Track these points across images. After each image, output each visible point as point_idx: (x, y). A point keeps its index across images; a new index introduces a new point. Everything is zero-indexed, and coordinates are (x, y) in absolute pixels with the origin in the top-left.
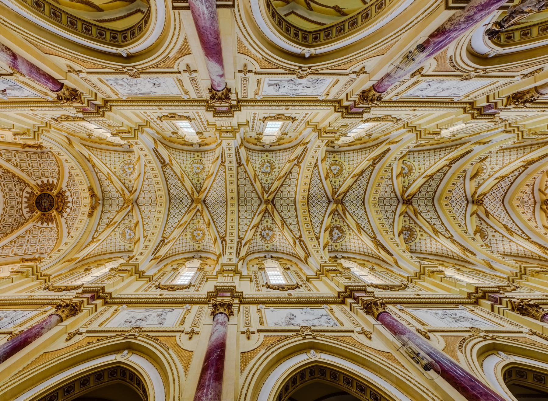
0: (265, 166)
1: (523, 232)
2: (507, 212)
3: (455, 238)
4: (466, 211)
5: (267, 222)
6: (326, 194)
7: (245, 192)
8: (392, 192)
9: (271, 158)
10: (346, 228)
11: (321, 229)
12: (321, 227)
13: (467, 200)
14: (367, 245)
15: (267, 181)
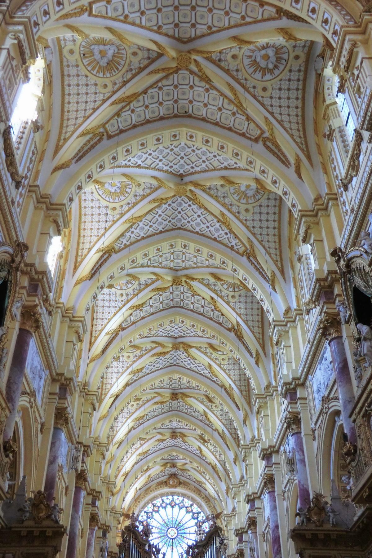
1: (142, 460)
3: (133, 431)
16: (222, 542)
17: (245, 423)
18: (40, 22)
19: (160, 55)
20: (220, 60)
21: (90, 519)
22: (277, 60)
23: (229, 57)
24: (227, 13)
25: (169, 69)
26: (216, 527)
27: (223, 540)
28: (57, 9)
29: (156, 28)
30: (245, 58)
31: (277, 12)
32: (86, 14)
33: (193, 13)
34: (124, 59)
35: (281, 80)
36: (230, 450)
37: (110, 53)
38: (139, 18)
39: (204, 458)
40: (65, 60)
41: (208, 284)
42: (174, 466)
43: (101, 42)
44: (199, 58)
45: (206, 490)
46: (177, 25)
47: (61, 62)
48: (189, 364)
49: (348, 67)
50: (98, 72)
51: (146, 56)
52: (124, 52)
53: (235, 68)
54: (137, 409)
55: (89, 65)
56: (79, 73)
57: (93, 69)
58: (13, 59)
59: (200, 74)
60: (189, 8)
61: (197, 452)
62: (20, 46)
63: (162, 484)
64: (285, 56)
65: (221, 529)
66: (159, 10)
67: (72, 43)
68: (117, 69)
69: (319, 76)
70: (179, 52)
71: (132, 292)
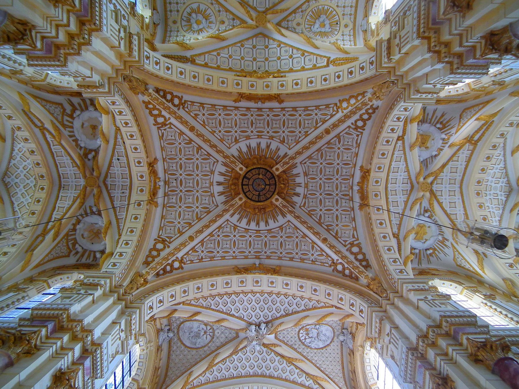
18: (368, 64)
19: (279, 24)
20: (234, 19)
22: (190, 20)
23: (227, 23)
24: (230, 57)
25: (273, 13)
28: (353, 69)
29: (282, 45)
30: (214, 22)
31: (194, 61)
32: (331, 59)
33: (255, 56)
34: (306, 20)
35: (184, 3)
37: (317, 26)
38: (294, 53)
40: (352, 20)
43: (324, 34)
44: (250, 22)
46: (267, 47)
47: (355, 18)
49: (130, 37)
50: (328, 10)
51: (290, 23)
52: (306, 26)
53: (221, 13)
55: (335, 16)
56: (342, 8)
57: (332, 12)
58: (397, 45)
59: (249, 9)
60: (258, 60)
62: (389, 54)
64: (184, 23)
66: (279, 58)
67: (345, 33)
68: (313, 12)
69: (154, 9)
70: (266, 28)
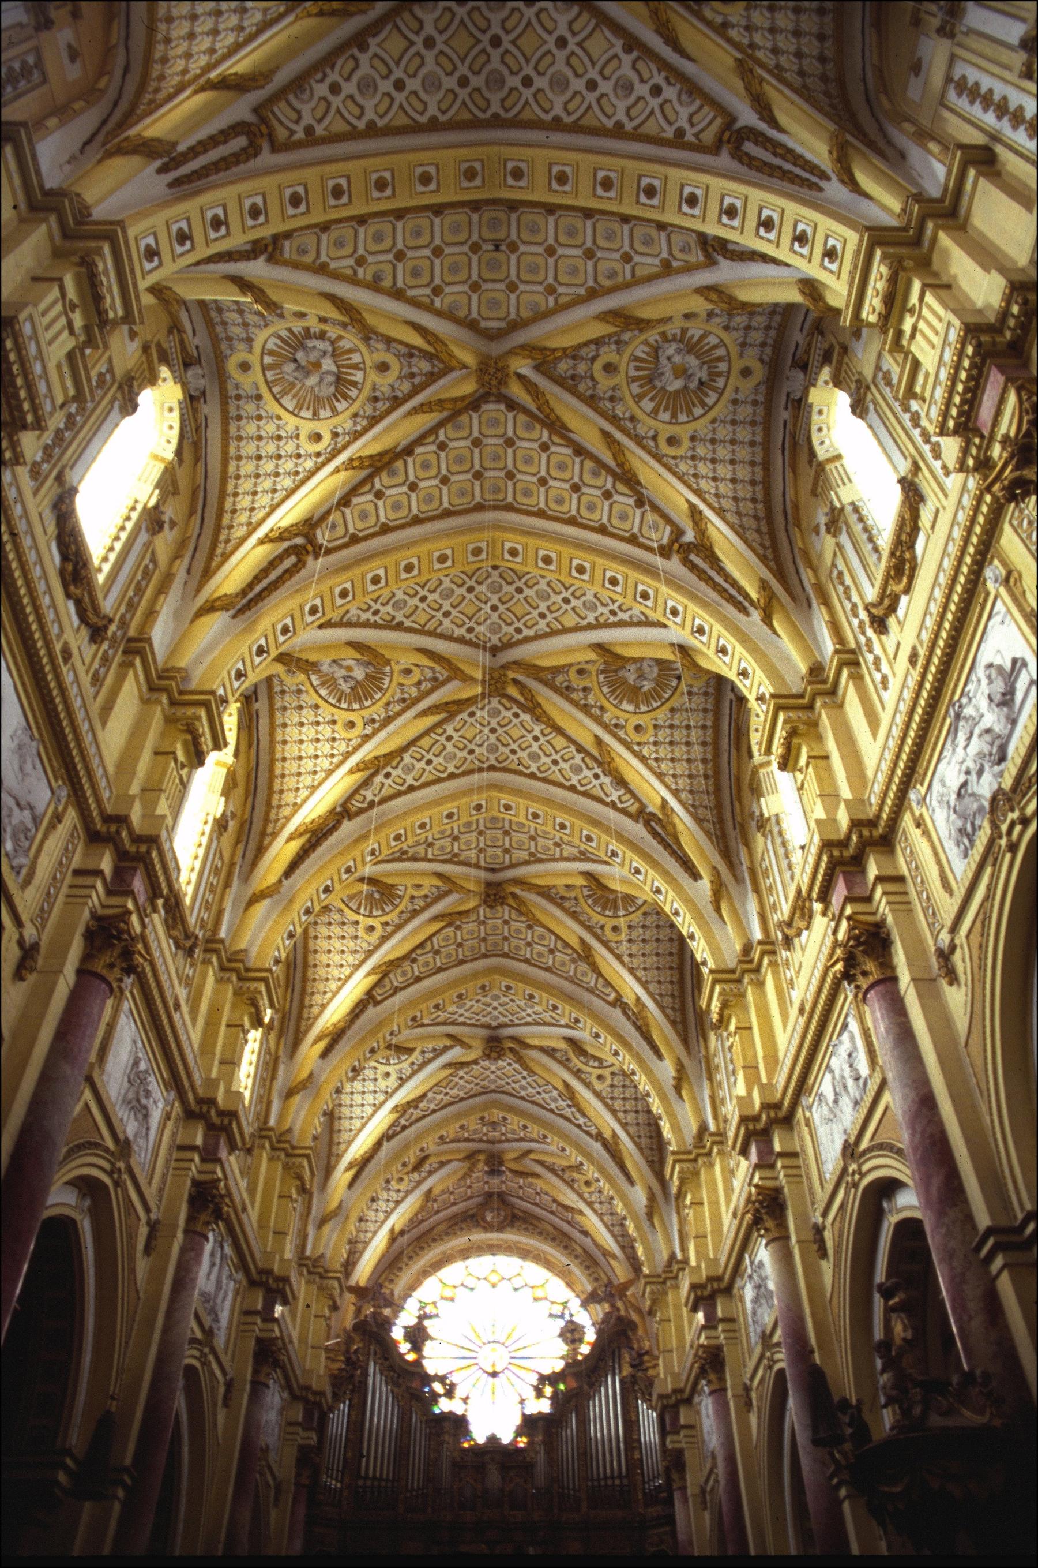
0: (693, 362)
1: (404, 1128)
2: (462, 1099)
3: (371, 1011)
4: (464, 1024)
5: (383, 367)
6: (527, 640)
7: (551, 251)
8: (532, 854)
9: (729, 394)
10: (376, 710)
11: (367, 625)
12: (376, 626)
13: (500, 1026)
14: (313, 789)
15: (610, 368)
16: (638, 1364)
17: (718, 910)
21: (192, 1201)
26: (620, 1319)
27: (640, 1355)
36: (660, 1057)
39: (581, 1121)
41: (592, 397)
42: (495, 1164)
45: (586, 1233)
48: (534, 757)
54: (384, 939)
61: (561, 1103)
63: (464, 1220)
65: (633, 1325)
71: (348, 425)
